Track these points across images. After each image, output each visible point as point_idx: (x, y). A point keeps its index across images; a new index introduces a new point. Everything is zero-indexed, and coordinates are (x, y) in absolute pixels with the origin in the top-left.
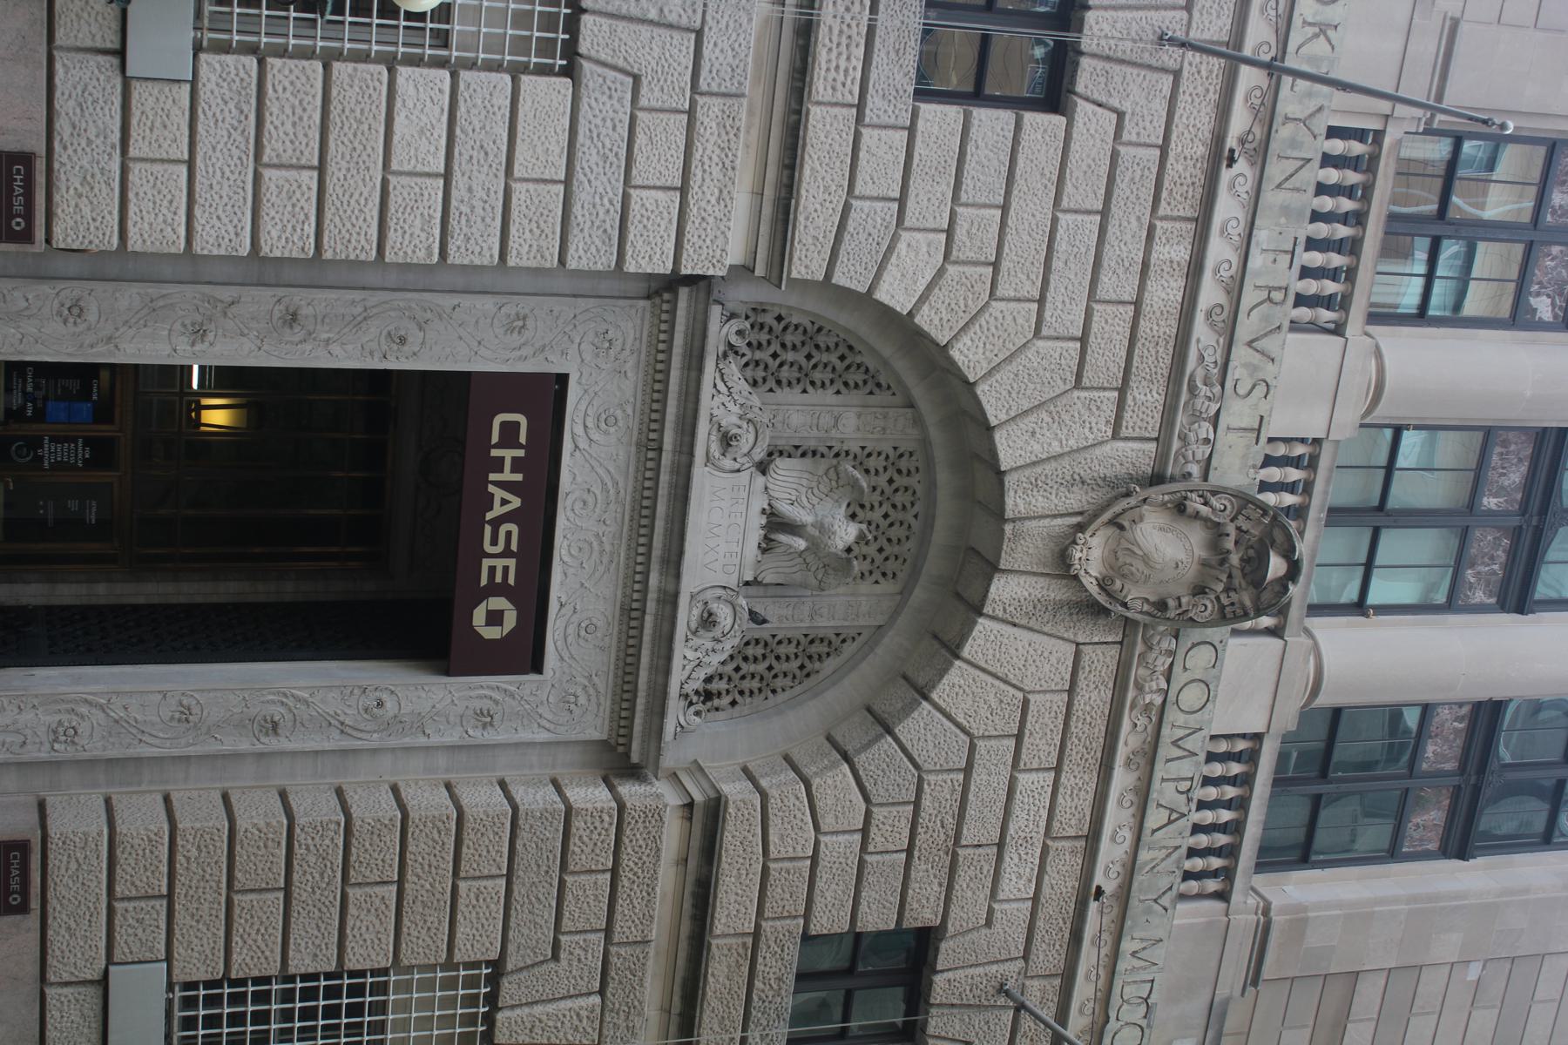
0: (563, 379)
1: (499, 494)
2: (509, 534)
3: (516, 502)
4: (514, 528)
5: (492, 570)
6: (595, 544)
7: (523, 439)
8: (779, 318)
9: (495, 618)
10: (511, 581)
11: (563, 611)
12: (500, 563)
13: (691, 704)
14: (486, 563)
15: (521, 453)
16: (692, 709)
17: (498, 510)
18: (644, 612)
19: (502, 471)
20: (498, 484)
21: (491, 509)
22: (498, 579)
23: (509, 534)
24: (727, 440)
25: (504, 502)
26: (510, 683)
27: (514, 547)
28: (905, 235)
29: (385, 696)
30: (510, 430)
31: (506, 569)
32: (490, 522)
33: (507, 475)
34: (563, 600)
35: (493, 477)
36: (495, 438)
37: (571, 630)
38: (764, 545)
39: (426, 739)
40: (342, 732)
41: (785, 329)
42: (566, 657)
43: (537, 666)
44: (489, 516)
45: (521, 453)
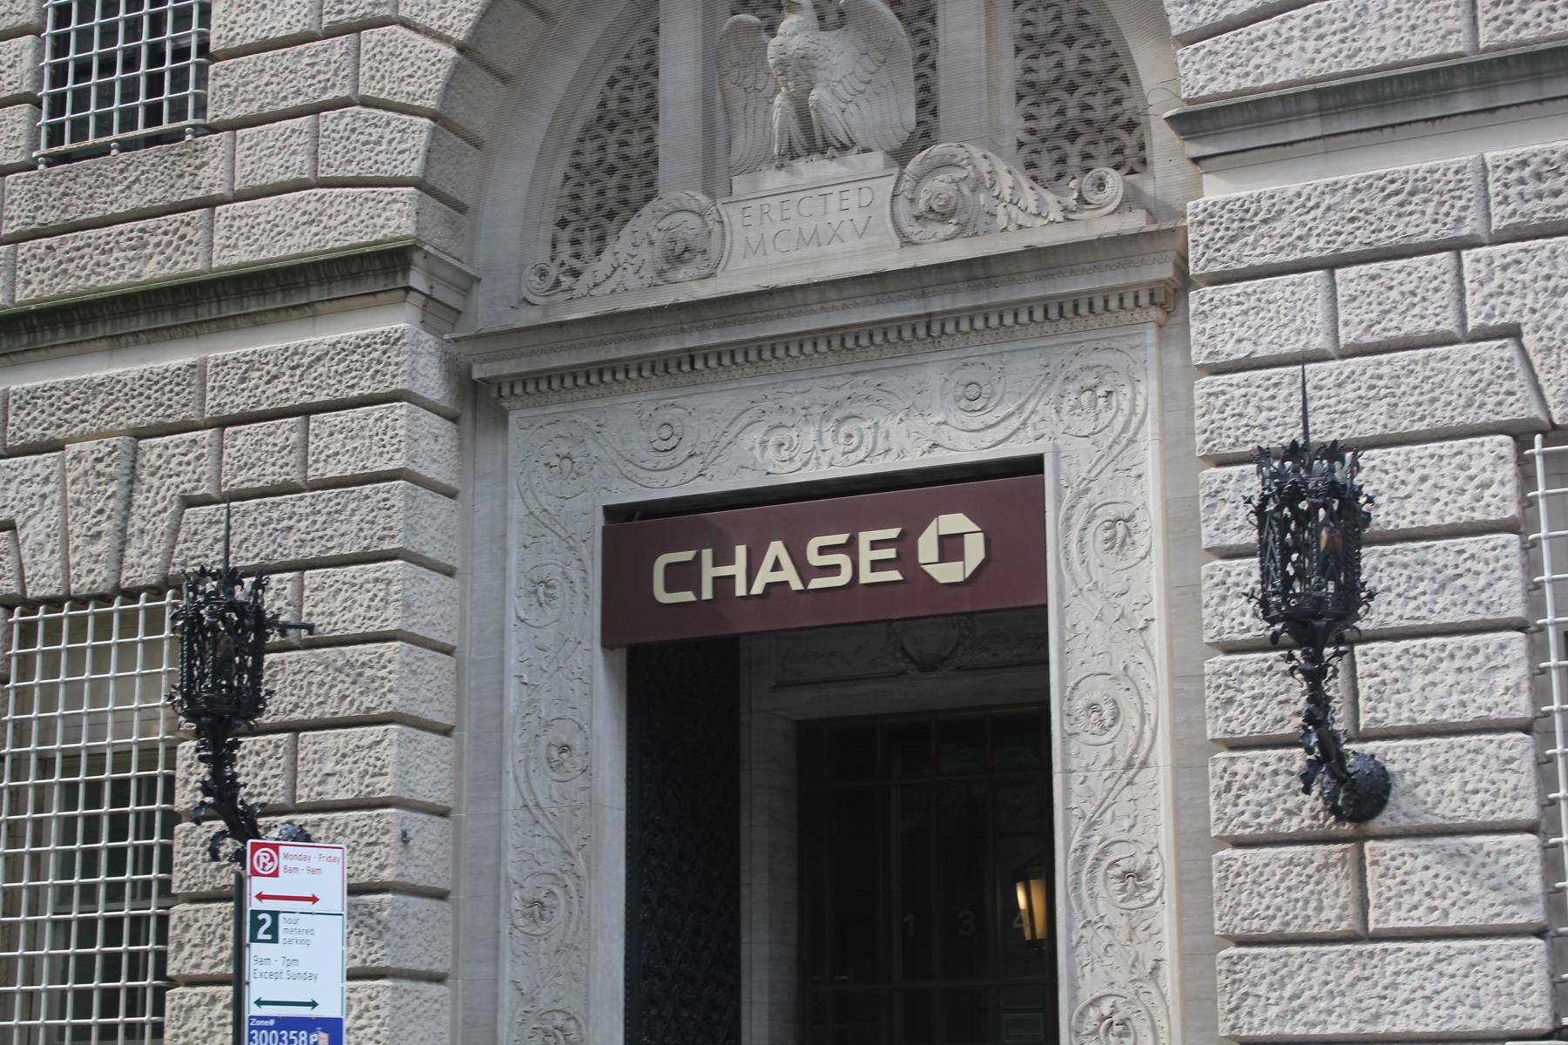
0: (610, 512)
1: (764, 576)
2: (823, 550)
3: (777, 549)
4: (814, 544)
5: (876, 565)
6: (839, 414)
7: (687, 556)
8: (563, 224)
9: (951, 547)
10: (893, 533)
11: (943, 440)
12: (866, 555)
13: (1081, 200)
14: (867, 577)
15: (707, 554)
16: (1091, 197)
17: (789, 574)
18: (930, 315)
19: (733, 577)
20: (750, 581)
21: (786, 583)
22: (890, 553)
23: (823, 550)
24: (678, 256)
25: (777, 566)
26: (1059, 502)
27: (841, 539)
28: (362, 91)
29: (1079, 704)
30: (683, 576)
31: (875, 545)
32: (805, 582)
33: (738, 569)
34: (926, 446)
35: (740, 590)
36: (688, 596)
37: (976, 421)
38: (830, 152)
39: (1154, 626)
40: (1144, 764)
41: (577, 211)
42: (1015, 422)
43: (1034, 465)
44: (796, 585)
45: (707, 554)
